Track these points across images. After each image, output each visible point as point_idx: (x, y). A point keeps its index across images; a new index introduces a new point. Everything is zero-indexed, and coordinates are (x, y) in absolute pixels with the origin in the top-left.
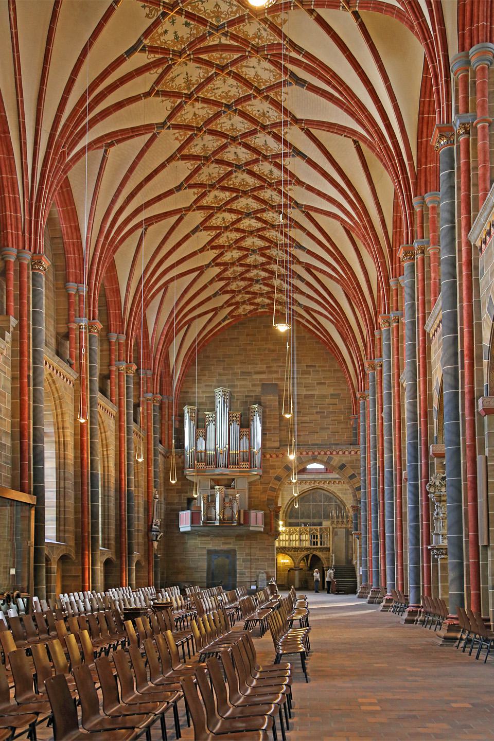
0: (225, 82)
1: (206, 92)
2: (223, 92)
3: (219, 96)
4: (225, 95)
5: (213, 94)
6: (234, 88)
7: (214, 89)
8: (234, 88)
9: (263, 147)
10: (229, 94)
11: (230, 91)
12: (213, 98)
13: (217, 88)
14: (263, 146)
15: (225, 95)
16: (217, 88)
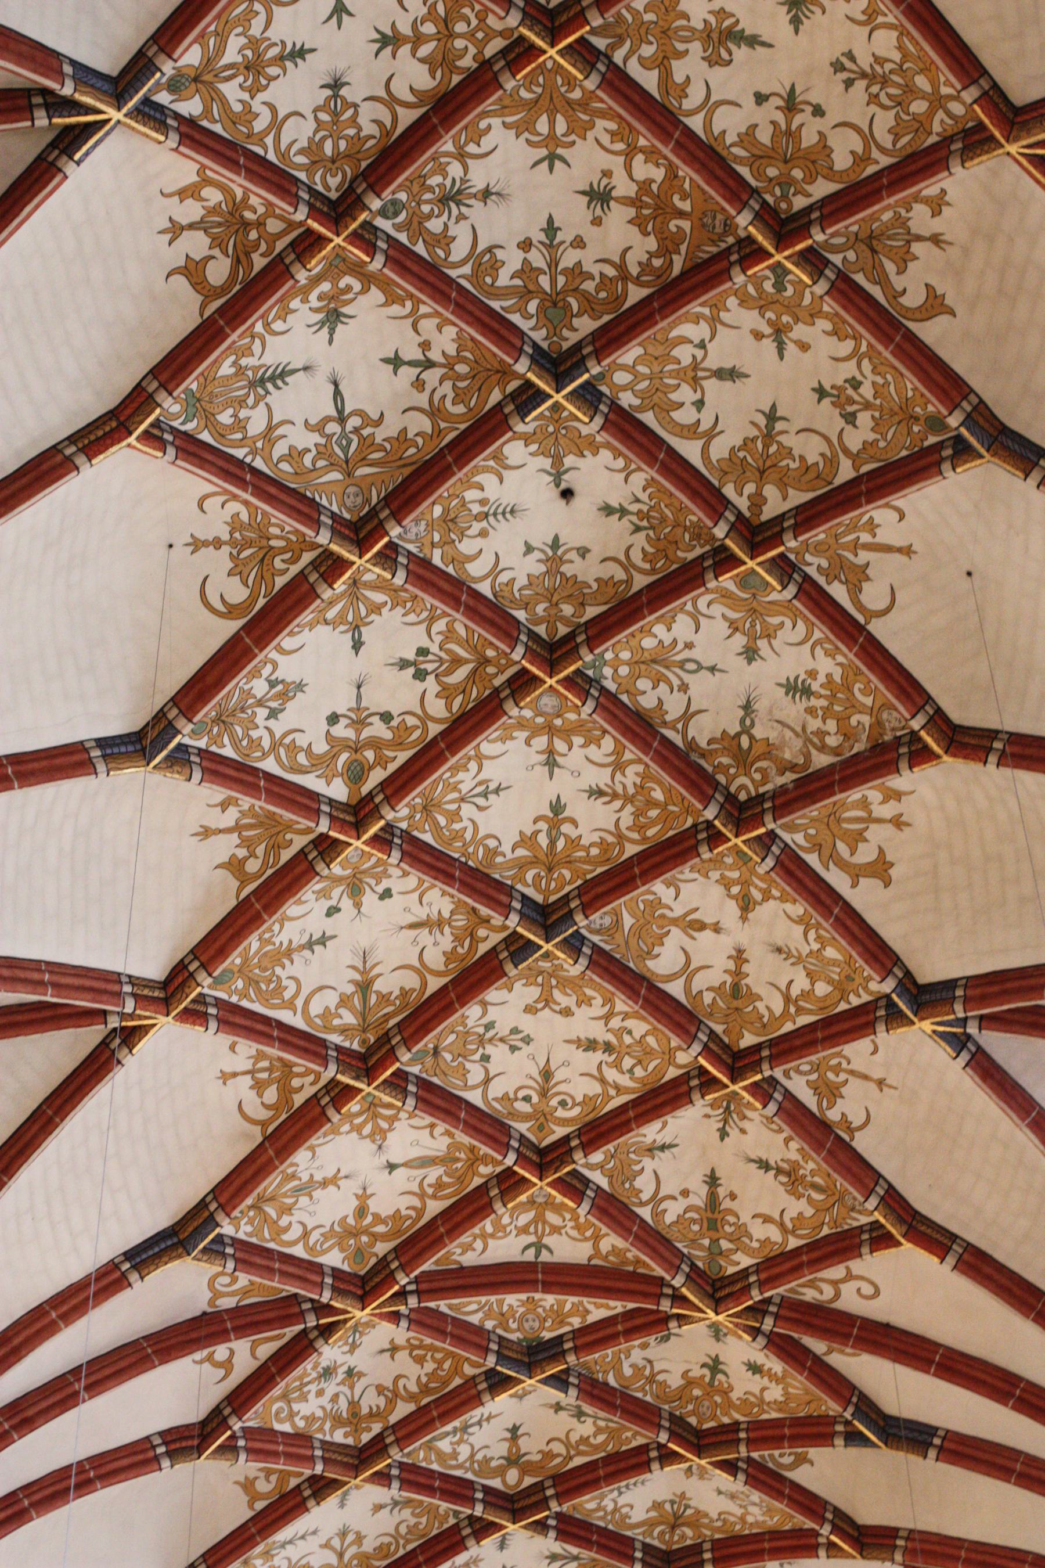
0: (547, 1074)
1: (649, 1052)
2: (567, 1012)
3: (588, 1001)
4: (557, 994)
5: (615, 1023)
6: (502, 1029)
7: (608, 1048)
8: (502, 1029)
9: (378, 597)
10: (534, 992)
11: (529, 1010)
12: (621, 1004)
13: (591, 1045)
14: (376, 609)
15: (557, 994)
16: (591, 1045)
